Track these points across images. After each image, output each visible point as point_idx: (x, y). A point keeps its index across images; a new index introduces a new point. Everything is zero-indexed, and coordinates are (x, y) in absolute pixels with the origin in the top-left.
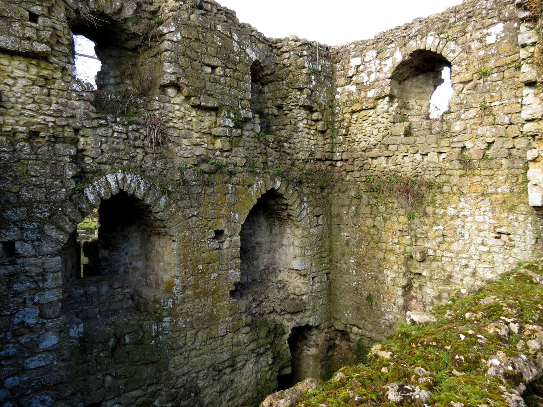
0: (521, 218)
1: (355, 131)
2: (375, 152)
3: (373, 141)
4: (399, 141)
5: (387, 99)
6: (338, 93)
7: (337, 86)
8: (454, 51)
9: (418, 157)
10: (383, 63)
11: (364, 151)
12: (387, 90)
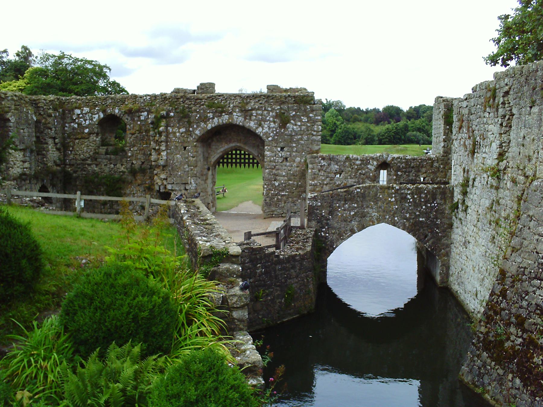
0: (155, 194)
1: (78, 149)
2: (89, 162)
3: (88, 155)
4: (103, 157)
5: (95, 135)
6: (66, 127)
7: (66, 123)
8: (127, 119)
9: (112, 166)
10: (93, 116)
11: (83, 160)
12: (96, 130)
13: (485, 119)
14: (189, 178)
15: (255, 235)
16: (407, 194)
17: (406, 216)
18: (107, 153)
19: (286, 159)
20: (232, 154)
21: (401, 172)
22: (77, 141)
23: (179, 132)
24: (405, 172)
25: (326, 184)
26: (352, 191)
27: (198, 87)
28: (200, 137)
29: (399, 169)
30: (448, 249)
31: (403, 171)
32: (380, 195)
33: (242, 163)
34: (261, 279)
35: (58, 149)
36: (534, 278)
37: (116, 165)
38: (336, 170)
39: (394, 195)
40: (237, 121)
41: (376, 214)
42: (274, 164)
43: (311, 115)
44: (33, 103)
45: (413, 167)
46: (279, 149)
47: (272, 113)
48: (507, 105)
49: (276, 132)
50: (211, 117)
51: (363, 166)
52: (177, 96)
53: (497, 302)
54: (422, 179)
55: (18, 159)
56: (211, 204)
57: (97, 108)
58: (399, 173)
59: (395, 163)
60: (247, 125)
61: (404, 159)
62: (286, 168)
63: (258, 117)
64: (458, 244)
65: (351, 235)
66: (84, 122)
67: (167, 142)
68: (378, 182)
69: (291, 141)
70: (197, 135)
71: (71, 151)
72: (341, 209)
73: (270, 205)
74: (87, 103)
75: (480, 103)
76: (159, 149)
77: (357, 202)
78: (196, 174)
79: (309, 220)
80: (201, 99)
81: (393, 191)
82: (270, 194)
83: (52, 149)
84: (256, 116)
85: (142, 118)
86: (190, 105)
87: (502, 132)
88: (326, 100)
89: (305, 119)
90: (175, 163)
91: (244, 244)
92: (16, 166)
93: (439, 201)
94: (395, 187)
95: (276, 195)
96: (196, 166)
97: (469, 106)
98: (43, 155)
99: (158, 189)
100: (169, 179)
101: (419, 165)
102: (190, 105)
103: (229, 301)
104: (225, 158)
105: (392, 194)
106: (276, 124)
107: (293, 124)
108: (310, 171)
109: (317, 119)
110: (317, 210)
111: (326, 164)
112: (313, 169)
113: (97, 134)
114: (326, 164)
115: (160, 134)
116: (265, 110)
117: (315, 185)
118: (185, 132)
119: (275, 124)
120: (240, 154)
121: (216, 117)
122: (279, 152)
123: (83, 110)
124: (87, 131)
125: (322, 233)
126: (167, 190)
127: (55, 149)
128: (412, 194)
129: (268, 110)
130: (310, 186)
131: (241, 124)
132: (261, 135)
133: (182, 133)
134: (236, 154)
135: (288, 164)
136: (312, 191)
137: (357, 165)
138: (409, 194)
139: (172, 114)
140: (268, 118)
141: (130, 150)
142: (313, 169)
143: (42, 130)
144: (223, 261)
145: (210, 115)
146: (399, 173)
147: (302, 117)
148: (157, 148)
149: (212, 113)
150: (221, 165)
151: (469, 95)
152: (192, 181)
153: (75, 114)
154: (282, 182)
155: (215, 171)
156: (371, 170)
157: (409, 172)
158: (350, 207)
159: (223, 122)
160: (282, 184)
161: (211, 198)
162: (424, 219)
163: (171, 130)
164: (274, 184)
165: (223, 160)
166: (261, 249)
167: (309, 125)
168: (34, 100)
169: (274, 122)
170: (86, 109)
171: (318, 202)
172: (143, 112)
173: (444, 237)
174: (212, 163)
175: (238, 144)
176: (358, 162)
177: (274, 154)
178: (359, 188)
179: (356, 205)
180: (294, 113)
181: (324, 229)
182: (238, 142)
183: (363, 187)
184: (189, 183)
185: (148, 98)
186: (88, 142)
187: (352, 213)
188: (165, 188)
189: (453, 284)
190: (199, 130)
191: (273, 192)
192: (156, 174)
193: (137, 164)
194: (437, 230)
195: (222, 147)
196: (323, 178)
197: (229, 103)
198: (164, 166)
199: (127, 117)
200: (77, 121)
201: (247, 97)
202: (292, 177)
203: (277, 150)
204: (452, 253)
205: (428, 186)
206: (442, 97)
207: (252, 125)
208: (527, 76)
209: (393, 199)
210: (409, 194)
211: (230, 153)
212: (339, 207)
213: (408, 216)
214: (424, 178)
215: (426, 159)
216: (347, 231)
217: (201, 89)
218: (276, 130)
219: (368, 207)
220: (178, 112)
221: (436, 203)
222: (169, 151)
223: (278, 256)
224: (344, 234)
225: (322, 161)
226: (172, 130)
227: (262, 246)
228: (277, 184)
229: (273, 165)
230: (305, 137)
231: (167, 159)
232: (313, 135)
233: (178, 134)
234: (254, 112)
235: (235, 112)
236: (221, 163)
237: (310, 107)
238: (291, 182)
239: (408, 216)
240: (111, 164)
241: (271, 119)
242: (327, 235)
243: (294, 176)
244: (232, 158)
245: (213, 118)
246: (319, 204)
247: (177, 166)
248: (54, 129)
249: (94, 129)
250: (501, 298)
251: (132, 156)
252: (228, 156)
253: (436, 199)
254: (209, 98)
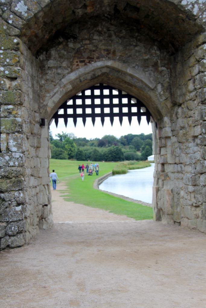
14: (3, 136)
70: (20, 16)
88: (63, 132)
132: (195, 11)
152: (12, 143)
175: (109, 63)
182: (109, 59)
211: (81, 94)
236: (61, 116)
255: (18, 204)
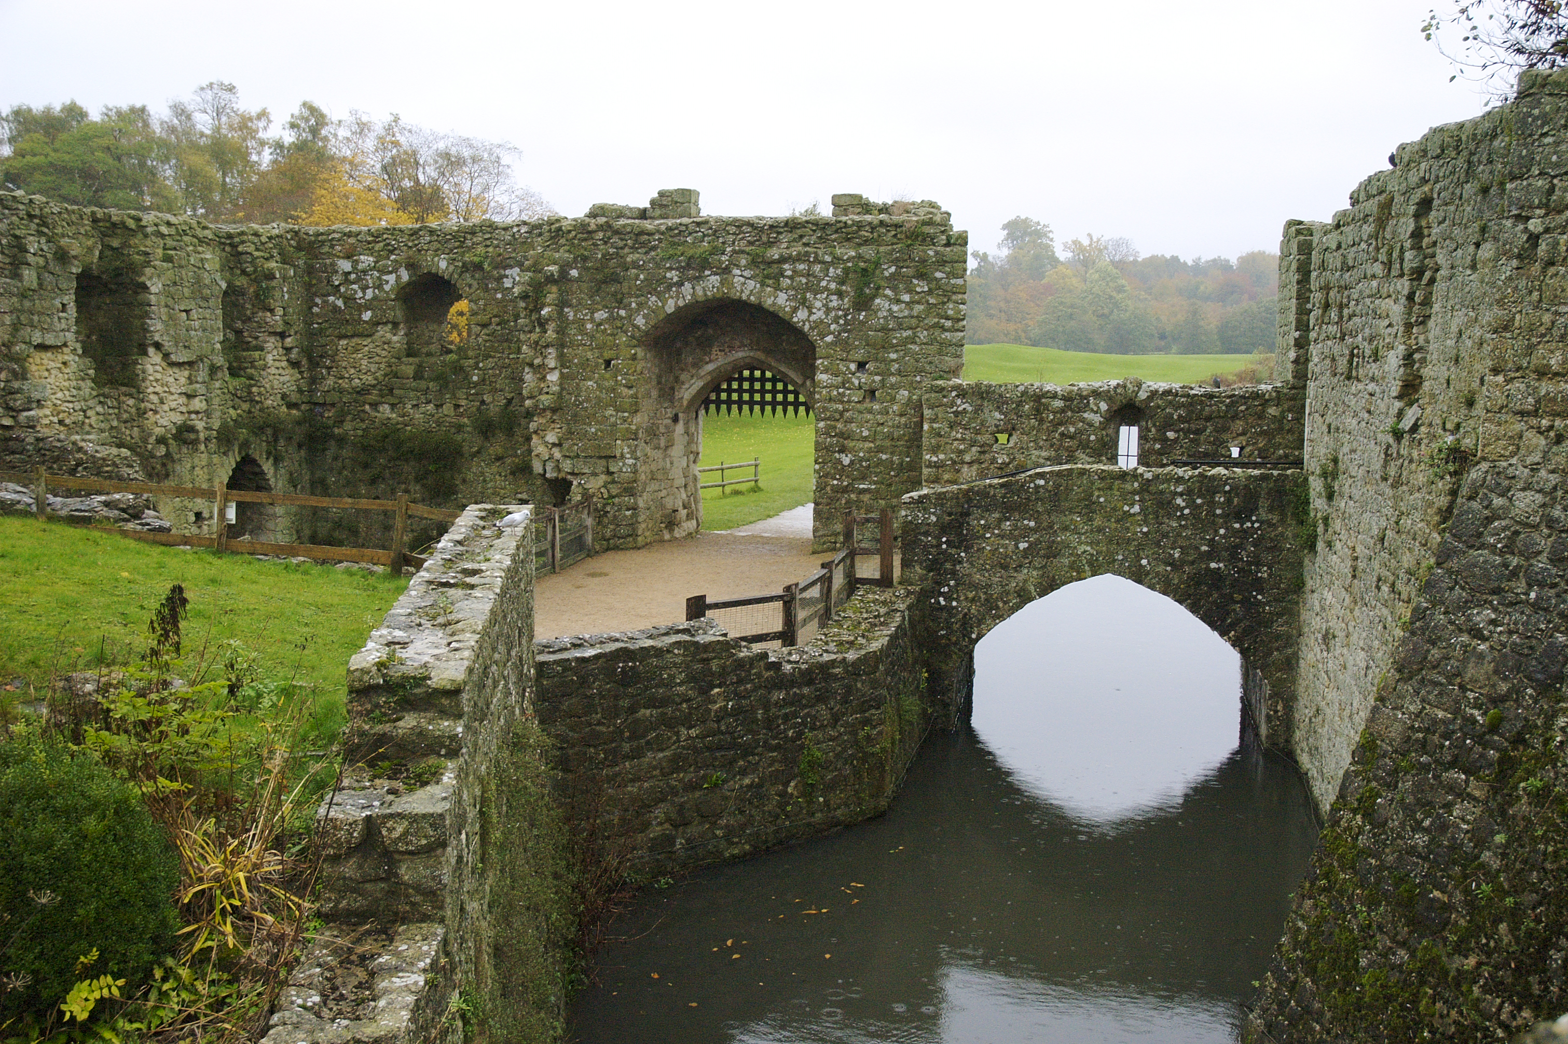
5: (390, 326)
6: (317, 305)
8: (470, 286)
10: (384, 277)
13: (1374, 283)
15: (717, 606)
16: (1176, 493)
17: (1171, 555)
18: (418, 376)
19: (872, 392)
20: (741, 379)
21: (1177, 431)
22: (344, 342)
23: (592, 320)
24: (1187, 432)
25: (970, 464)
26: (1022, 486)
27: (653, 202)
28: (647, 333)
29: (1168, 424)
30: (1290, 651)
31: (1182, 430)
32: (1099, 497)
33: (791, 403)
34: (723, 728)
35: (295, 364)
36: (1452, 765)
37: (441, 405)
38: (996, 426)
39: (1137, 498)
40: (742, 291)
41: (1088, 548)
42: (840, 407)
43: (938, 275)
44: (224, 244)
45: (1208, 419)
46: (853, 367)
47: (836, 268)
48: (1426, 240)
49: (846, 320)
50: (676, 279)
51: (1069, 414)
52: (588, 224)
53: (1349, 828)
54: (1235, 452)
55: (173, 390)
56: (683, 513)
57: (393, 257)
58: (1171, 435)
59: (1159, 407)
60: (770, 301)
61: (1182, 396)
62: (869, 416)
63: (798, 279)
64: (1313, 637)
65: (1019, 607)
66: (360, 294)
67: (561, 345)
68: (1114, 459)
69: (886, 346)
70: (638, 328)
71: (329, 368)
72: (993, 533)
73: (828, 519)
74: (369, 243)
75: (1365, 238)
76: (543, 366)
77: (1036, 516)
78: (636, 434)
79: (905, 564)
80: (650, 234)
81: (1136, 485)
82: (828, 488)
83: (277, 364)
84: (791, 278)
85: (508, 283)
86: (622, 248)
87: (1413, 320)
89: (922, 286)
90: (581, 403)
91: (678, 632)
92: (166, 407)
93: (1264, 516)
94: (1142, 475)
95: (845, 490)
96: (636, 411)
97: (1344, 246)
98: (250, 378)
99: (541, 471)
100: (566, 445)
101: (1227, 411)
102: (622, 248)
103: (384, 832)
104: (724, 390)
105: (1134, 493)
106: (846, 300)
107: (890, 300)
108: (926, 427)
109: (954, 286)
110: (926, 534)
111: (970, 409)
112: (933, 421)
113: (395, 325)
114: (970, 409)
115: (542, 323)
116: (817, 261)
117: (938, 466)
118: (612, 319)
119: (842, 300)
120: (763, 380)
121: (688, 280)
122: (853, 374)
123: (357, 262)
124: (367, 316)
125: (941, 599)
126: (561, 476)
127: (284, 364)
128: (1189, 492)
129: (823, 262)
130: (927, 467)
131: (752, 298)
133: (600, 324)
134: (752, 379)
135: (876, 407)
136: (933, 482)
137: (1054, 413)
138: (1181, 494)
139: (574, 273)
140: (824, 283)
141: (477, 368)
142: (933, 421)
143: (248, 312)
144: (410, 704)
145: (673, 275)
146: (1171, 435)
147: (915, 282)
148: (537, 361)
149: (677, 269)
150: (713, 407)
151: (1344, 213)
152: (626, 450)
153: (337, 272)
154: (861, 454)
155: (697, 424)
156: (1091, 425)
157: (1198, 432)
158: (1016, 527)
159: (706, 295)
160: (861, 460)
161: (684, 496)
162: (1221, 565)
163: (572, 314)
164: (839, 461)
165: (718, 396)
166: (726, 646)
167: (932, 301)
168: (230, 236)
169: (840, 294)
170: (366, 260)
171: (930, 513)
172: (511, 267)
173: (1280, 615)
174: (685, 403)
176: (1058, 404)
177: (840, 379)
178: (1041, 475)
179: (1032, 524)
180: (893, 269)
181: (946, 589)
183: (1051, 472)
184: (618, 455)
185: (524, 229)
186: (371, 345)
187: (1023, 546)
188: (558, 468)
189: (1299, 751)
190: (644, 316)
191: (835, 482)
192: (535, 432)
193: (495, 404)
194: (1259, 597)
195: (711, 361)
196: (962, 447)
197: (723, 243)
198: (554, 411)
199: (469, 281)
200: (342, 289)
201: (771, 227)
202: (888, 443)
203: (848, 368)
204: (1301, 661)
205: (1234, 472)
206: (1300, 223)
207: (781, 301)
208: (1472, 154)
209: (1136, 509)
210: (1181, 494)
212: (987, 528)
213: (1177, 555)
214: (1242, 449)
215: (1243, 397)
216: (1008, 593)
217: (662, 206)
218: (846, 315)
219: (1065, 529)
220: (588, 269)
221: (1257, 521)
222: (566, 371)
223: (777, 666)
224: (1001, 604)
225: (959, 402)
226: (575, 315)
227: (732, 635)
228: (846, 461)
229: (836, 411)
230: (923, 335)
231: (560, 393)
232: (944, 329)
233: (589, 326)
234: (786, 266)
235: (738, 266)
236: (713, 402)
237: (937, 253)
238: (884, 457)
239: (1177, 555)
240: (429, 402)
241: (833, 286)
242: (954, 604)
243: (893, 439)
244: (740, 391)
245: (680, 284)
246: (934, 518)
247: (586, 409)
248: (280, 311)
249: (385, 311)
250: (1358, 817)
251: (483, 381)
252: (729, 385)
253: (1257, 509)
254: (670, 229)
255: (628, 509)
